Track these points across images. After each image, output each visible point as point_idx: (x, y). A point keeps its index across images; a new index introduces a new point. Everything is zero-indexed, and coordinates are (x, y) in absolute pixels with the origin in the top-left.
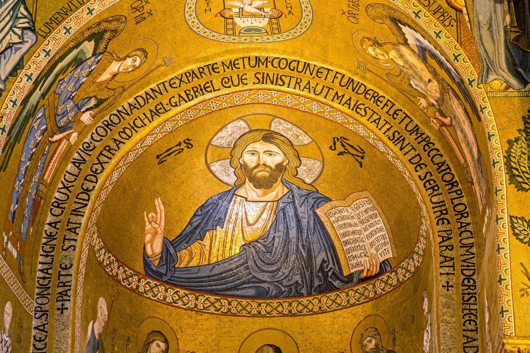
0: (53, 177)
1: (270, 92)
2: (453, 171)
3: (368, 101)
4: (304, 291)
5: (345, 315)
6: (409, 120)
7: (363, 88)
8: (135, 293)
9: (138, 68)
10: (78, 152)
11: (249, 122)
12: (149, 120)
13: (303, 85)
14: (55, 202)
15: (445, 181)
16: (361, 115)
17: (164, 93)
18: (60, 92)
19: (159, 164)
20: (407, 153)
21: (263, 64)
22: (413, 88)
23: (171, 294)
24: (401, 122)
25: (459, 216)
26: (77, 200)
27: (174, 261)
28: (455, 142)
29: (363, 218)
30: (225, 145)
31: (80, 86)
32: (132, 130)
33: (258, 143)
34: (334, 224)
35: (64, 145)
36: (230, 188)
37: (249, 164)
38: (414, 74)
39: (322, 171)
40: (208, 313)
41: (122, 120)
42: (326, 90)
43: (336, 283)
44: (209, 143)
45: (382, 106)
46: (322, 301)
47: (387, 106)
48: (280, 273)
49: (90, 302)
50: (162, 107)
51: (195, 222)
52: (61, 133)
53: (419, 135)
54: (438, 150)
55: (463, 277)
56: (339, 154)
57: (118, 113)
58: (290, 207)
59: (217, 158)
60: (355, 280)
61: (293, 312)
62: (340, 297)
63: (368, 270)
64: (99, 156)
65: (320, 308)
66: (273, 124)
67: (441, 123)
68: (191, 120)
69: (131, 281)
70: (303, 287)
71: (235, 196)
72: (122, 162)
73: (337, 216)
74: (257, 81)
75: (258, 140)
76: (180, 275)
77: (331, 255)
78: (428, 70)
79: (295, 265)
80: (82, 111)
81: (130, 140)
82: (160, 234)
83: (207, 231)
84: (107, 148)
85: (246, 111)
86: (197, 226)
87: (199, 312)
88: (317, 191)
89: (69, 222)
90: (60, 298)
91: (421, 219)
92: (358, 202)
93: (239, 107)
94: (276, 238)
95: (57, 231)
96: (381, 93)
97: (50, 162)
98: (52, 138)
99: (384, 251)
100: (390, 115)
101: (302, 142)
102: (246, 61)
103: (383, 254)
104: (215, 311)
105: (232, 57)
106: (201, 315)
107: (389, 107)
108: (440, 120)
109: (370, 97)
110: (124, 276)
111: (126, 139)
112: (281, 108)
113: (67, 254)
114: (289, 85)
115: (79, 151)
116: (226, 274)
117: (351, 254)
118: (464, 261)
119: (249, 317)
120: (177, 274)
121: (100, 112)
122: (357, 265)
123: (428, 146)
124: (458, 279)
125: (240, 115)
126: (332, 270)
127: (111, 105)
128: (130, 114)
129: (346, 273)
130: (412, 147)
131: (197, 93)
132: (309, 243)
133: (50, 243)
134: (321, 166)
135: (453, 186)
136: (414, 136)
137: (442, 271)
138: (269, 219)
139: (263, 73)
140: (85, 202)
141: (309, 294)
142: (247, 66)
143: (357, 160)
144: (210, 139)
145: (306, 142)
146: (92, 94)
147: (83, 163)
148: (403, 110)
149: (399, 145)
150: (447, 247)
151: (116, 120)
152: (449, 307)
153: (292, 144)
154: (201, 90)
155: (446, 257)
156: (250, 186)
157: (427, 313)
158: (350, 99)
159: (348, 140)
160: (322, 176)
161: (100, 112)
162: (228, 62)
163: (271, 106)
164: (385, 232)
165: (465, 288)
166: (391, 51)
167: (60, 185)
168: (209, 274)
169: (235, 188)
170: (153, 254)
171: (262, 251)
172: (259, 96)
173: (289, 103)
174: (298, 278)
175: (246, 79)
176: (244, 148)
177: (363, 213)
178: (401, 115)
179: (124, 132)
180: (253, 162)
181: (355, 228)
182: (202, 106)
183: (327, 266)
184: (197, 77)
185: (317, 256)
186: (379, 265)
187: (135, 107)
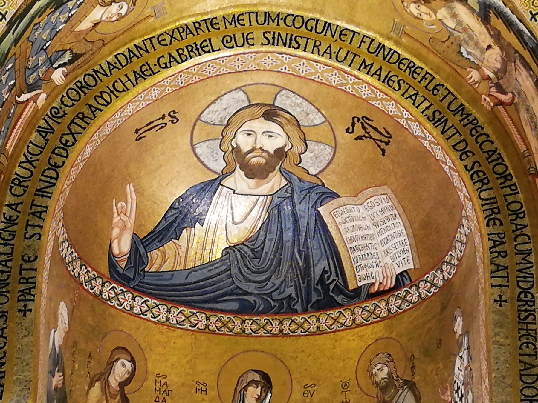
0: (15, 147)
1: (281, 56)
4: (298, 307)
7: (396, 56)
8: (99, 299)
9: (123, 17)
10: (44, 119)
11: (248, 94)
13: (322, 49)
14: (16, 179)
16: (394, 89)
17: (152, 51)
19: (136, 140)
21: (273, 21)
22: (464, 56)
23: (140, 304)
25: (514, 217)
26: (43, 178)
27: (143, 263)
31: (56, 34)
33: (256, 120)
34: (340, 226)
35: (31, 108)
36: (217, 176)
37: (242, 148)
38: (467, 39)
39: (332, 159)
40: (181, 329)
41: (99, 81)
42: (350, 57)
43: (339, 299)
44: (198, 118)
46: (321, 319)
47: (426, 79)
48: (270, 284)
50: (148, 68)
52: (29, 92)
53: (464, 116)
54: (488, 136)
55: (519, 290)
56: (356, 139)
57: (94, 73)
58: (287, 203)
61: (284, 332)
63: (380, 283)
64: (70, 124)
65: (318, 328)
68: (182, 87)
69: (94, 285)
70: (297, 302)
71: (220, 186)
72: (97, 133)
73: (345, 216)
74: (267, 41)
76: (149, 281)
77: (334, 264)
78: (489, 33)
79: (289, 275)
80: (54, 66)
82: (130, 229)
84: (81, 116)
85: (247, 79)
86: (174, 221)
87: (171, 327)
88: (323, 185)
89: (32, 205)
90: (22, 298)
91: (461, 219)
92: (373, 198)
96: (418, 63)
97: (14, 128)
98: (19, 97)
100: (430, 91)
101: (312, 121)
102: (253, 16)
104: (191, 326)
105: (237, 11)
106: (174, 331)
107: (427, 81)
108: (496, 98)
109: (405, 68)
110: (87, 278)
111: (104, 105)
114: (305, 48)
115: (46, 118)
118: (520, 271)
120: (146, 280)
121: (73, 70)
123: (476, 130)
124: (512, 292)
126: (335, 282)
127: (86, 62)
128: (109, 74)
130: (457, 130)
131: (192, 54)
132: (308, 248)
133: (9, 229)
134: (332, 153)
135: (506, 180)
136: (458, 117)
138: (260, 217)
139: (274, 33)
140: (52, 181)
141: (305, 311)
142: (254, 23)
143: (379, 146)
145: (317, 122)
147: (50, 133)
148: (445, 85)
149: (441, 128)
150: (499, 253)
151: (92, 82)
152: (501, 327)
154: (197, 49)
155: (498, 265)
156: (240, 174)
157: (460, 335)
158: (380, 69)
159: (372, 121)
160: (331, 166)
161: (73, 70)
163: (279, 73)
164: (406, 237)
165: (521, 303)
166: (441, 9)
167: (23, 159)
168: (183, 281)
170: (120, 253)
172: (266, 61)
174: (291, 291)
175: (253, 39)
177: (379, 213)
179: (102, 97)
180: (247, 145)
182: (196, 69)
183: (329, 277)
184: (192, 33)
185: (317, 264)
187: (115, 67)
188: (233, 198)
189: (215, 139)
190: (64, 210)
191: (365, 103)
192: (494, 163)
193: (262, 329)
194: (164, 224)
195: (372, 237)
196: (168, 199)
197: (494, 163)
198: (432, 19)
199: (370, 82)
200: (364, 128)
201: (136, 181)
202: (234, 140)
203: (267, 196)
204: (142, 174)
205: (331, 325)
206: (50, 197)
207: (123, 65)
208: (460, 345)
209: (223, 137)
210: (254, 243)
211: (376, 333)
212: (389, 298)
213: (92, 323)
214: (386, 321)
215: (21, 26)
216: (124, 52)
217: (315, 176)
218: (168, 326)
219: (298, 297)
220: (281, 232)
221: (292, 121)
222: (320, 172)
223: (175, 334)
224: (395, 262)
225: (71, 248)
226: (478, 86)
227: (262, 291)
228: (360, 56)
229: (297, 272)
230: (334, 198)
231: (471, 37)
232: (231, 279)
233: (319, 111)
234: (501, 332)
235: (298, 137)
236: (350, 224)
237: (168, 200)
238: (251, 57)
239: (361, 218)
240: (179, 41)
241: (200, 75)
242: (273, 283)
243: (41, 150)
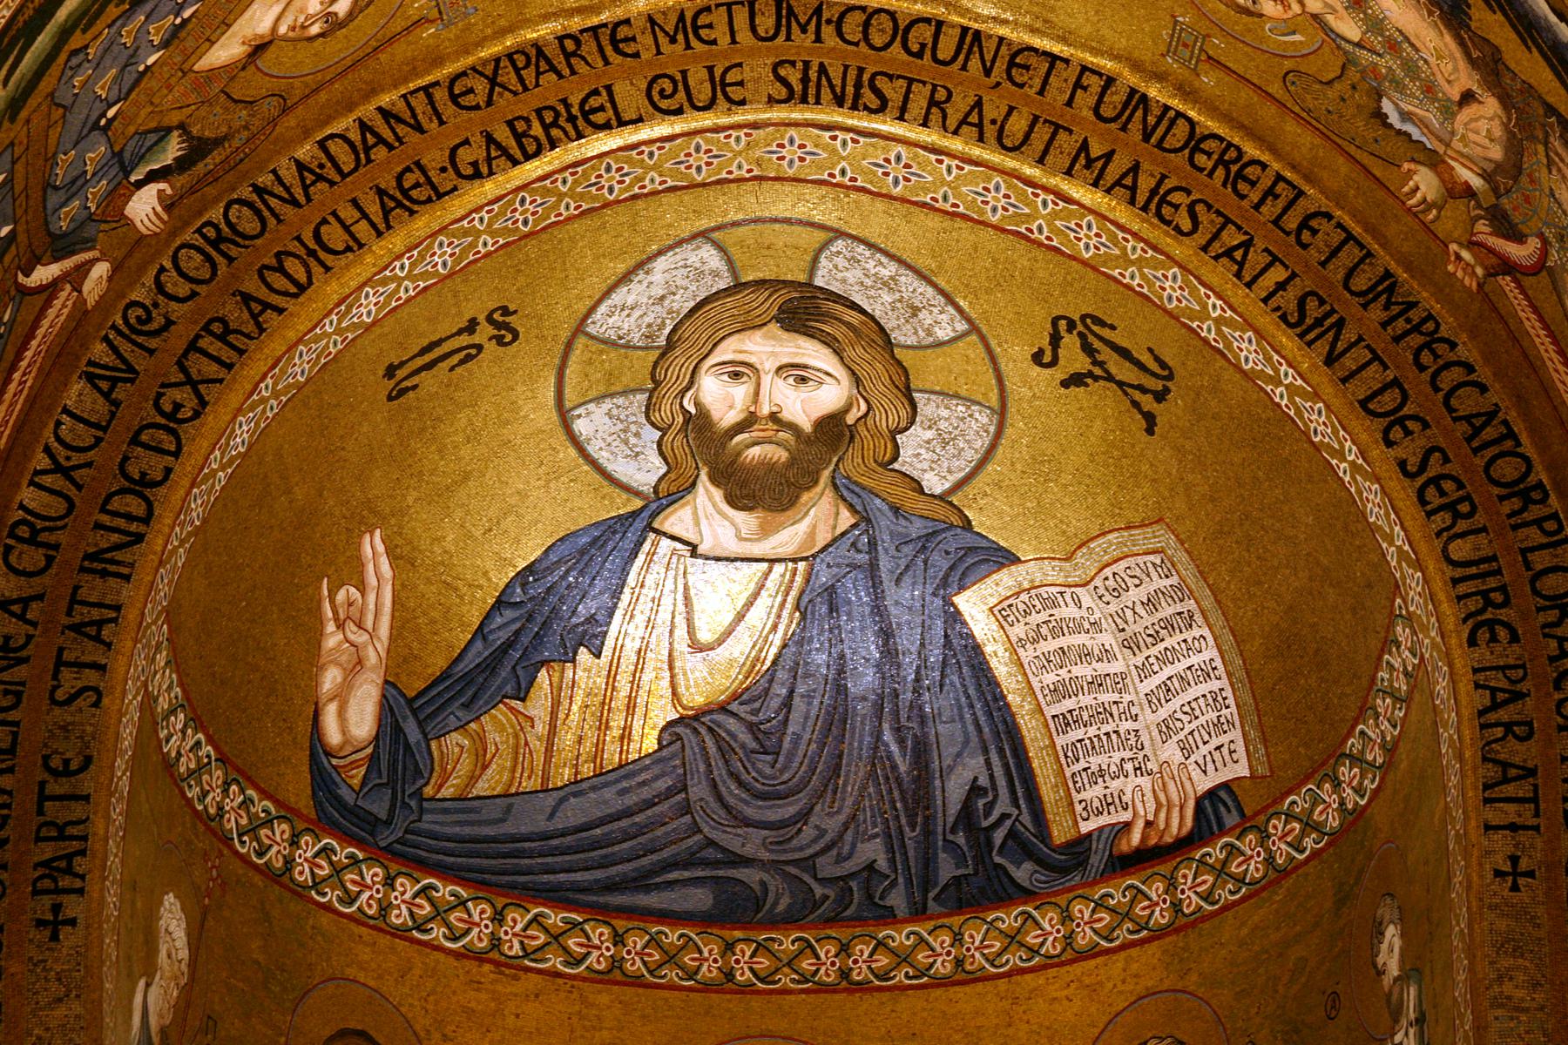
1: (827, 134)
2: (1528, 448)
3: (1203, 177)
4: (897, 900)
5: (1054, 991)
6: (1358, 253)
7: (1181, 129)
8: (282, 885)
10: (106, 339)
11: (732, 250)
12: (373, 225)
13: (957, 108)
15: (1497, 483)
16: (1178, 229)
18: (67, 102)
19: (390, 398)
20: (1353, 374)
21: (804, 30)
22: (1391, 126)
23: (407, 896)
24: (1328, 260)
26: (105, 519)
27: (418, 773)
28: (1551, 334)
29: (1138, 628)
30: (636, 338)
31: (137, 82)
32: (312, 262)
33: (758, 335)
34: (1021, 651)
35: (64, 306)
36: (638, 503)
41: (272, 222)
42: (1041, 134)
43: (1023, 873)
44: (579, 329)
45: (1255, 197)
46: (966, 937)
47: (1277, 197)
48: (808, 832)
49: (139, 904)
50: (422, 180)
51: (499, 628)
52: (56, 260)
53: (1396, 309)
54: (1470, 369)
56: (1065, 384)
57: (255, 197)
59: (602, 389)
60: (1097, 860)
61: (855, 977)
62: (1037, 923)
63: (1148, 824)
64: (185, 354)
65: (959, 962)
66: (823, 261)
67: (1494, 260)
68: (526, 236)
70: (894, 884)
71: (652, 536)
72: (269, 381)
73: (1035, 619)
74: (784, 91)
75: (758, 321)
76: (437, 828)
77: (1006, 766)
78: (1467, 54)
80: (133, 179)
81: (302, 299)
82: (373, 669)
83: (543, 663)
84: (217, 328)
86: (509, 644)
88: (967, 525)
89: (74, 601)
91: (1390, 627)
92: (1123, 564)
93: (704, 192)
94: (797, 700)
95: (31, 630)
96: (1251, 150)
98: (27, 276)
99: (1217, 755)
100: (1288, 234)
101: (929, 333)
103: (1210, 767)
104: (567, 963)
107: (1281, 203)
108: (1491, 251)
109: (1210, 164)
110: (244, 821)
111: (286, 294)
112: (865, 198)
113: (69, 719)
116: (606, 829)
117: (1082, 764)
119: (690, 989)
120: (428, 823)
122: (1107, 803)
123: (1433, 352)
125: (704, 223)
126: (1008, 823)
128: (302, 200)
129: (1060, 833)
130: (1372, 351)
131: (555, 132)
134: (992, 429)
135: (1527, 501)
136: (1376, 313)
137: (1493, 815)
138: (775, 628)
139: (807, 64)
140: (134, 527)
141: (919, 913)
142: (744, 36)
143: (1135, 404)
144: (584, 311)
145: (943, 333)
146: (175, 118)
149: (1323, 346)
150: (1508, 727)
151: (249, 225)
152: (1518, 952)
153: (888, 344)
154: (572, 119)
155: (1505, 765)
156: (711, 498)
157: (1396, 979)
158: (1135, 169)
159: (1113, 328)
160: (990, 467)
161: (192, 190)
162: (673, 19)
163: (824, 190)
164: (1225, 682)
167: (42, 461)
168: (542, 825)
169: (654, 506)
170: (346, 742)
171: (743, 746)
172: (784, 152)
173: (896, 182)
174: (873, 851)
175: (741, 84)
176: (705, 351)
177: (1139, 609)
178: (1327, 234)
179: (281, 270)
180: (731, 407)
181: (1103, 668)
182: (570, 179)
183: (989, 808)
184: (553, 68)
185: (951, 768)
186: (1191, 804)
187: (320, 178)
188: (690, 570)
189: (634, 391)
190: (170, 614)
191: (1091, 274)
192: (1489, 453)
193: (786, 970)
194: (480, 652)
195: (1119, 682)
196: (491, 574)
197: (1489, 453)
198: (1290, 14)
199: (1103, 210)
200: (1088, 349)
201: (393, 521)
202: (689, 394)
203: (794, 560)
204: (410, 500)
205: (999, 954)
206: (127, 578)
207: (346, 169)
208: (1396, 1013)
209: (657, 383)
210: (757, 705)
211: (1136, 976)
212: (1176, 868)
213: (261, 958)
214: (1168, 939)
215: (28, 55)
216: (347, 129)
217: (940, 497)
218: (497, 964)
219: (896, 871)
220: (841, 672)
221: (865, 330)
222: (959, 486)
223: (517, 987)
224: (1192, 759)
225: (196, 731)
226: (1437, 218)
227: (785, 851)
228: (1071, 132)
229: (890, 791)
230: (1001, 566)
231: (1411, 68)
232: (687, 818)
233: (950, 300)
234: (1518, 968)
235: (887, 382)
236: (1051, 645)
237: (489, 580)
238: (738, 139)
239: (1087, 626)
240: (515, 93)
241: (582, 199)
242: (817, 827)
243: (100, 434)
